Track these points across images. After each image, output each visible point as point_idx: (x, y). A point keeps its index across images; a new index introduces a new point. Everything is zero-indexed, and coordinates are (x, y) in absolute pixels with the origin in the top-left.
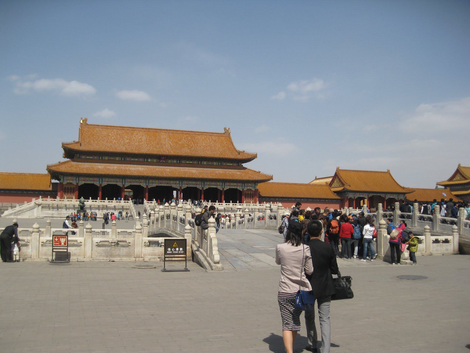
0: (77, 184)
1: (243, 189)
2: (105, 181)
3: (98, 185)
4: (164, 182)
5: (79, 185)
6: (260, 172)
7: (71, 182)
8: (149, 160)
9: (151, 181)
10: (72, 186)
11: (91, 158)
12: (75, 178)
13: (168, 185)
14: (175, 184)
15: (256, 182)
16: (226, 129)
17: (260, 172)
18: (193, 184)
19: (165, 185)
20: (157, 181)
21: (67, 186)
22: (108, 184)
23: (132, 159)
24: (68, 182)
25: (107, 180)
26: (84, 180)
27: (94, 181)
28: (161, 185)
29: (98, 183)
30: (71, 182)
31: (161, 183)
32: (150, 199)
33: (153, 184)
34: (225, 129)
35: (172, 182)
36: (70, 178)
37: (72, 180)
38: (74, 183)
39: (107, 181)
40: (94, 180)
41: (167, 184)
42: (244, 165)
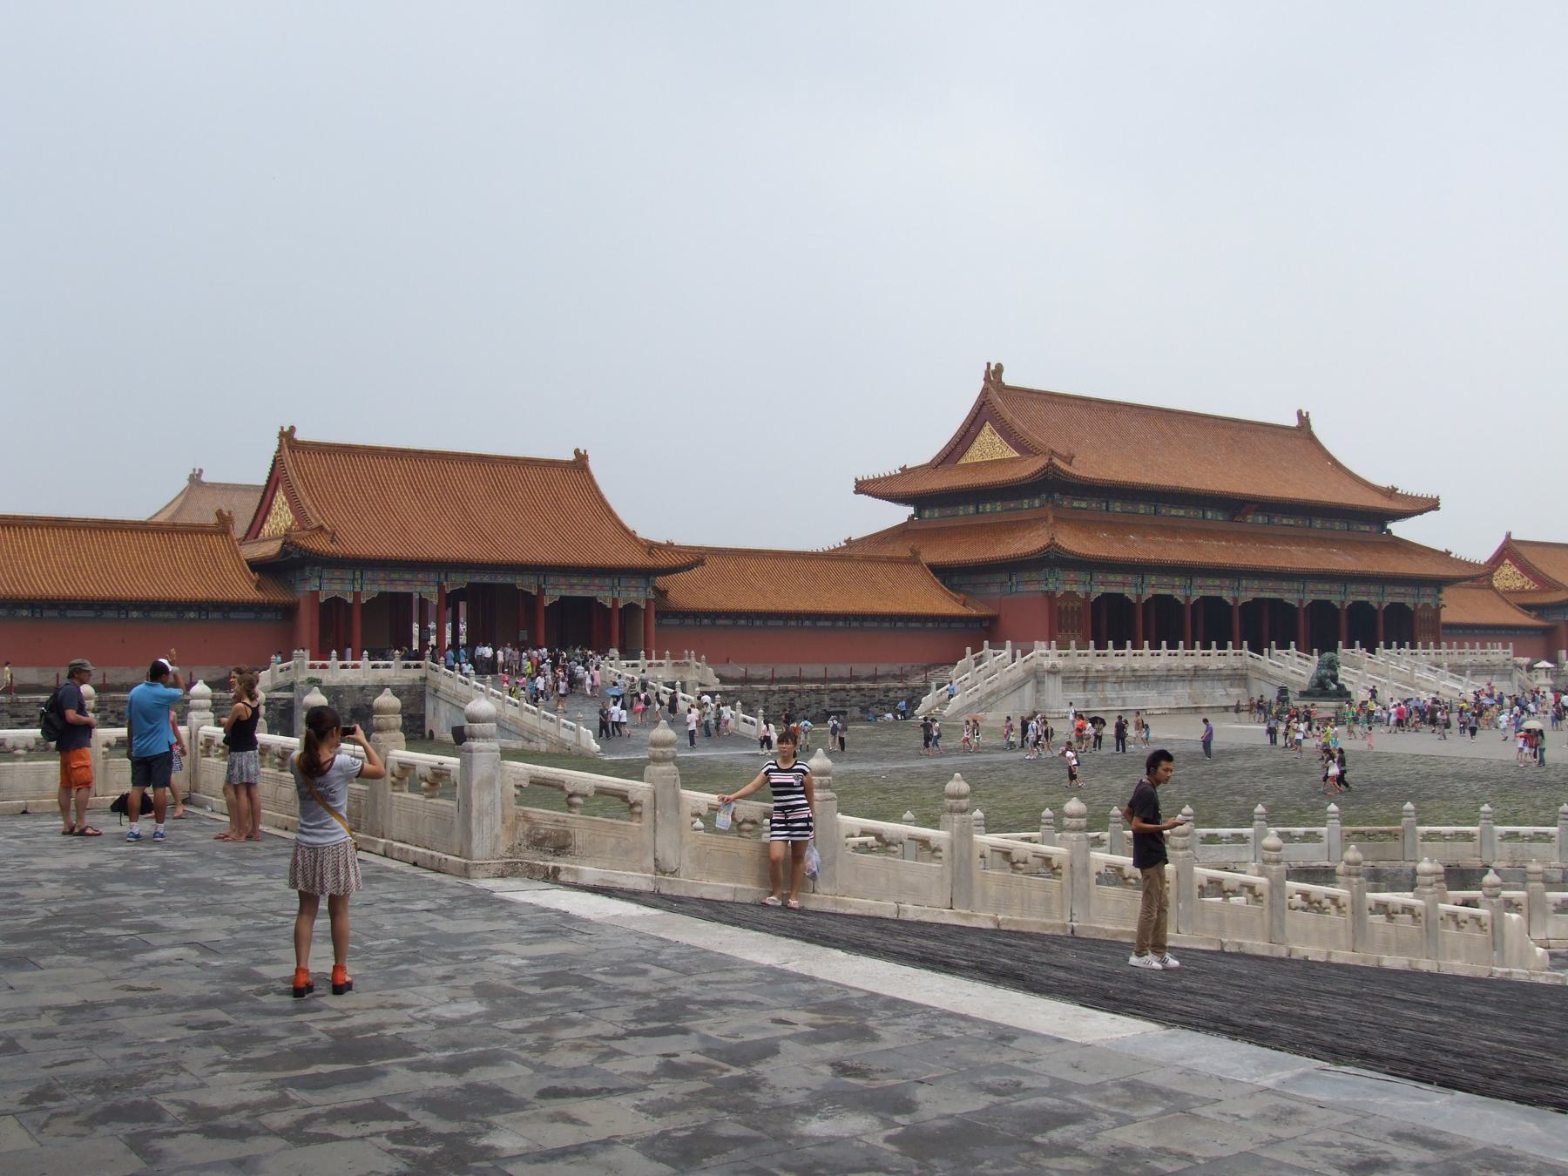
0: (1088, 595)
6: (1448, 553)
8: (1209, 515)
9: (1244, 583)
11: (1084, 505)
15: (1439, 583)
18: (1324, 592)
20: (1256, 584)
23: (1173, 512)
24: (1068, 588)
27: (1124, 584)
28: (1262, 595)
32: (1350, 645)
33: (1249, 593)
34: (1300, 413)
35: (1285, 585)
42: (1398, 529)
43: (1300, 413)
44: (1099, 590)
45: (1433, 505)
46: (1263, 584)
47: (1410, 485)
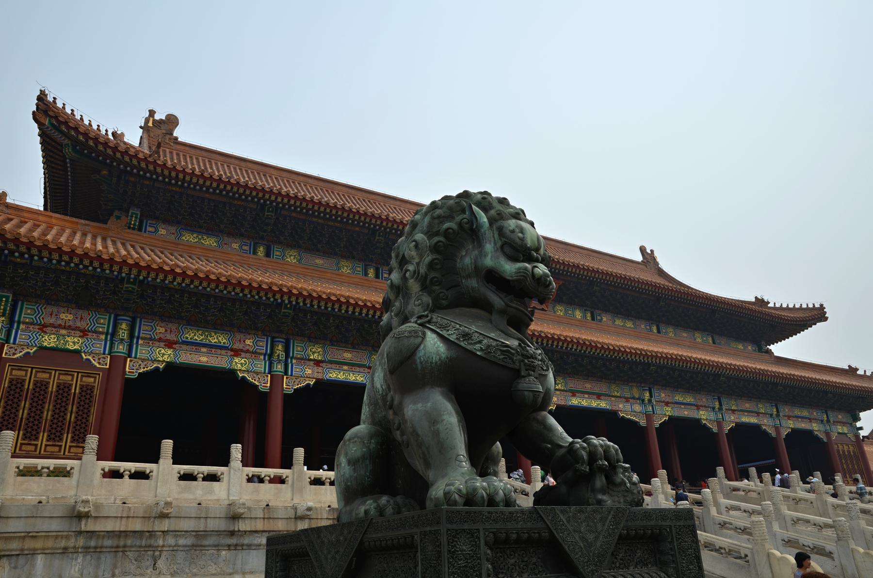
1: (828, 434)
2: (304, 360)
3: (264, 384)
4: (588, 386)
5: (133, 369)
7: (71, 347)
10: (76, 383)
12: (103, 323)
13: (603, 404)
14: (627, 400)
16: (645, 249)
17: (857, 369)
19: (594, 404)
21: (29, 377)
22: (319, 382)
24: (49, 341)
25: (315, 356)
26: (170, 344)
27: (237, 353)
28: (575, 401)
29: (261, 365)
30: (73, 343)
31: (574, 394)
34: (642, 250)
36: (66, 317)
37: (84, 333)
38: (96, 353)
39: (318, 363)
40: (238, 346)
41: (599, 396)
42: (779, 349)
43: (642, 250)
44: (153, 355)
45: (818, 315)
46: (572, 384)
47: (781, 296)
